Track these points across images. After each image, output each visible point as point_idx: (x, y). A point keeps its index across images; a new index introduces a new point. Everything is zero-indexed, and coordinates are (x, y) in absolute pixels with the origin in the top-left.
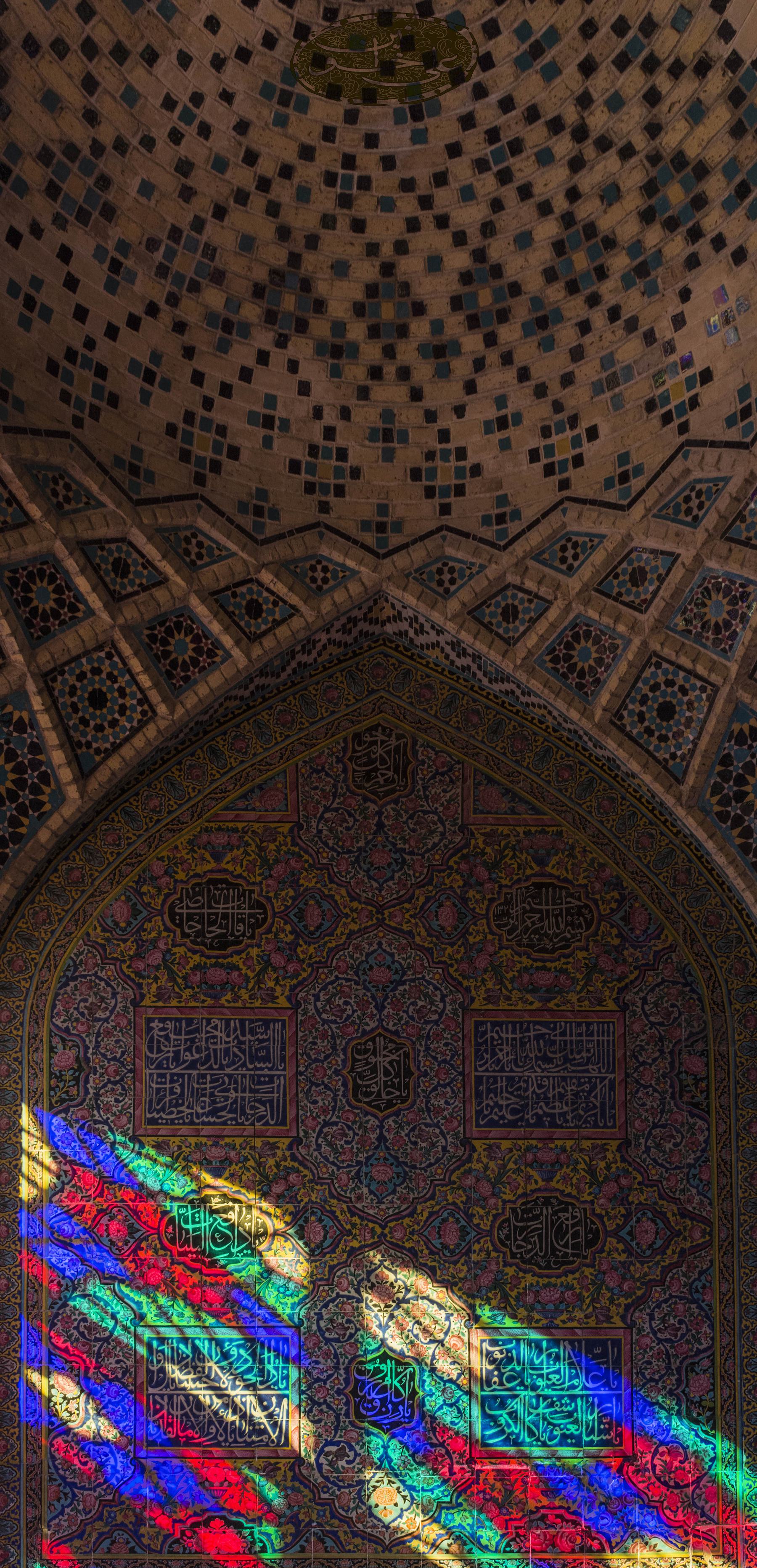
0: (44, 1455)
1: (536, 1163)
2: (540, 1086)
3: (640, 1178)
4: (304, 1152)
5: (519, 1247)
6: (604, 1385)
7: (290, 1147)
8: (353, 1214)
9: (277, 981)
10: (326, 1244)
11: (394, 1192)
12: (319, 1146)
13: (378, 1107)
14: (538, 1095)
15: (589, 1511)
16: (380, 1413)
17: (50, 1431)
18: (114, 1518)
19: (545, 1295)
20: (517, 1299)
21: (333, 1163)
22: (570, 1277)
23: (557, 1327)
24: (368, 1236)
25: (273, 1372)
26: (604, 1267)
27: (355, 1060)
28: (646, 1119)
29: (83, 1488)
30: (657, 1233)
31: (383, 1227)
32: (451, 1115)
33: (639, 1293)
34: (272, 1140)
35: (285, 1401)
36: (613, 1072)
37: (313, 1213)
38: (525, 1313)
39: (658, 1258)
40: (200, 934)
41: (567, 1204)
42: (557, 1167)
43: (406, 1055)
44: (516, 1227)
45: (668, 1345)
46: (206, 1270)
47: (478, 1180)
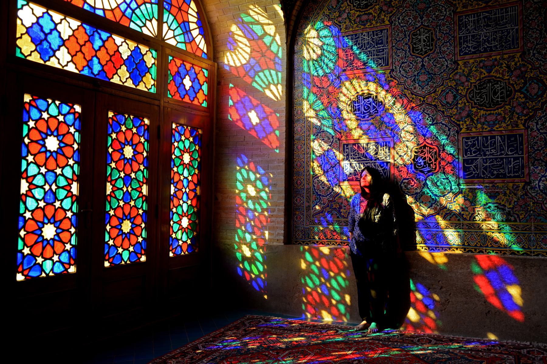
1: (485, 67)
2: (485, 37)
4: (395, 74)
5: (477, 100)
6: (516, 153)
7: (390, 73)
8: (412, 94)
9: (385, 16)
11: (428, 85)
12: (400, 71)
13: (421, 54)
14: (485, 40)
15: (510, 204)
16: (423, 167)
19: (489, 118)
20: (477, 121)
21: (405, 77)
22: (500, 110)
23: (494, 130)
24: (418, 102)
26: (515, 105)
27: (413, 38)
28: (533, 42)
30: (539, 88)
31: (424, 98)
32: (449, 53)
33: (531, 114)
36: (518, 25)
39: (540, 99)
40: (359, 4)
41: (498, 81)
42: (493, 67)
43: (432, 33)
44: (476, 93)
46: (362, 119)
47: (460, 76)
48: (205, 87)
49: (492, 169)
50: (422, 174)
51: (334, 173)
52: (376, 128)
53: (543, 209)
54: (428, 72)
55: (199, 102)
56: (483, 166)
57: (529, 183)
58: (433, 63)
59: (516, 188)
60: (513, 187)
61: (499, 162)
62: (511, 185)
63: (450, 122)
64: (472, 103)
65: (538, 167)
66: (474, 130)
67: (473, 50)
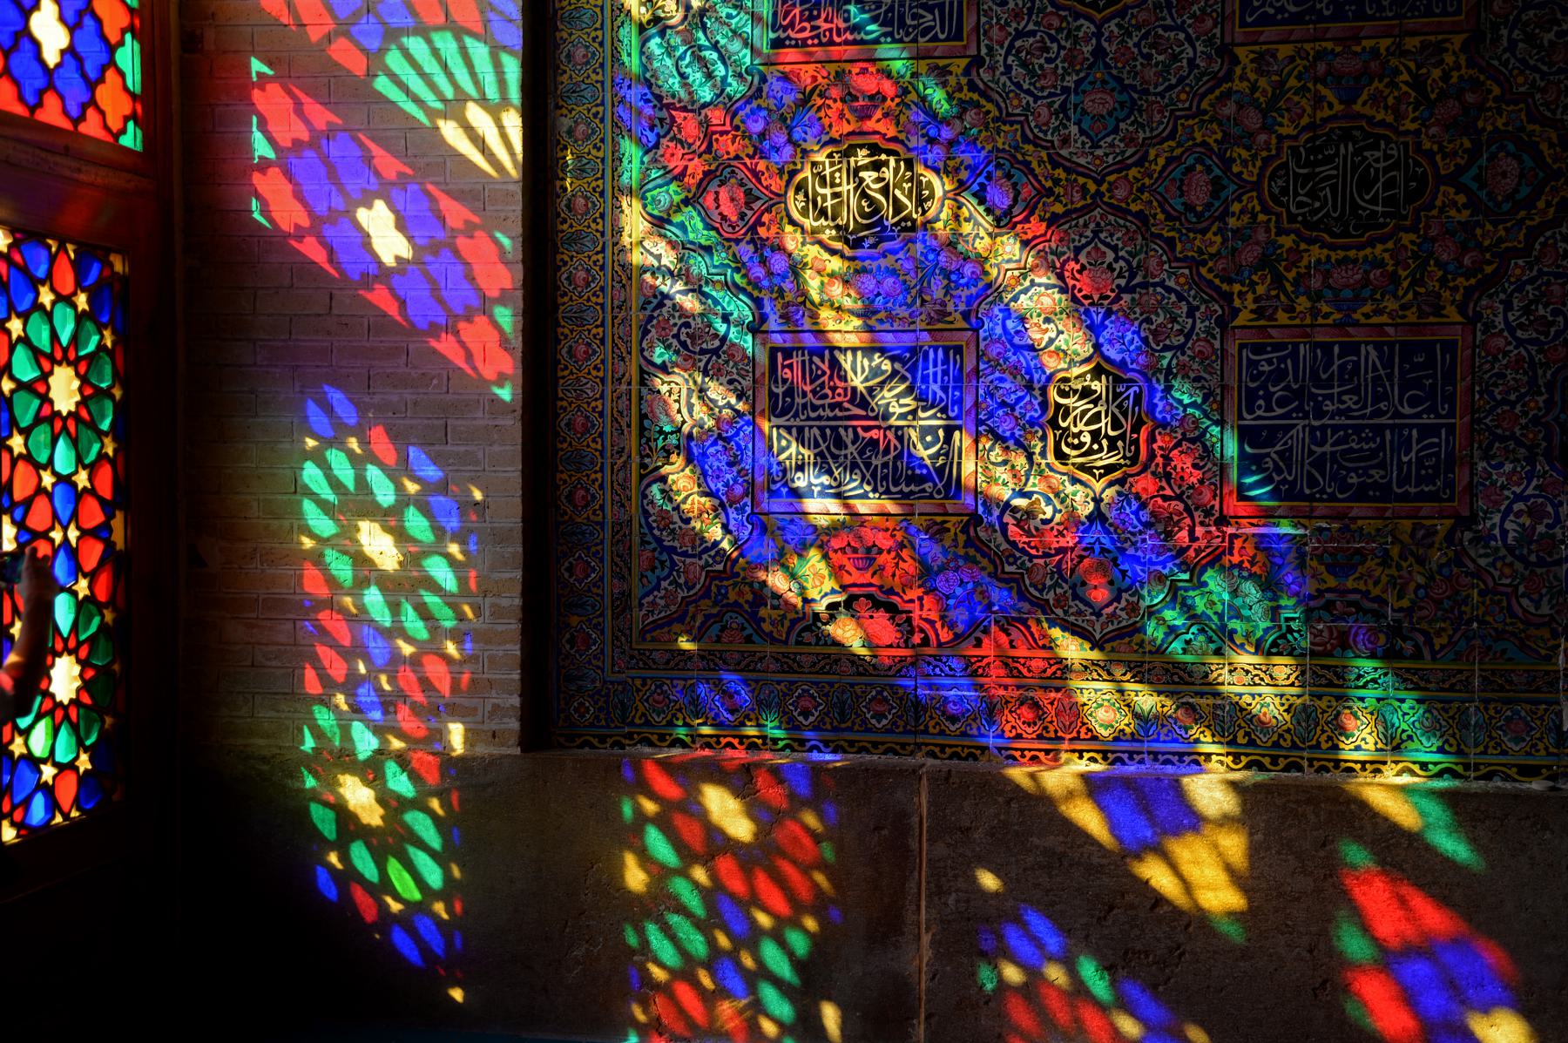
0: (634, 509)
3: (1497, 91)
4: (986, 77)
6: (1428, 411)
7: (967, 72)
8: (1055, 165)
10: (1016, 211)
11: (1116, 130)
12: (1008, 68)
15: (1400, 597)
16: (1090, 452)
17: (642, 477)
18: (725, 596)
20: (1296, 283)
21: (1028, 92)
22: (1380, 247)
23: (1356, 324)
24: (1077, 196)
25: (940, 393)
26: (1433, 232)
29: (685, 554)
30: (1522, 175)
32: (1202, 10)
33: (1488, 269)
34: (942, 63)
35: (957, 434)
37: (999, 166)
38: (1309, 305)
39: (1523, 213)
41: (1379, 137)
45: (1533, 349)
47: (1240, 107)
48: (128, 57)
49: (1341, 467)
50: (1084, 477)
51: (730, 464)
52: (908, 290)
53: (1513, 615)
54: (1119, 80)
55: (106, 128)
56: (1311, 453)
57: (1470, 521)
58: (1137, 45)
59: (1424, 537)
60: (1412, 535)
61: (1367, 440)
62: (1407, 524)
63: (1197, 282)
64: (1279, 216)
65: (1501, 465)
66: (1282, 317)
67: (1293, 9)
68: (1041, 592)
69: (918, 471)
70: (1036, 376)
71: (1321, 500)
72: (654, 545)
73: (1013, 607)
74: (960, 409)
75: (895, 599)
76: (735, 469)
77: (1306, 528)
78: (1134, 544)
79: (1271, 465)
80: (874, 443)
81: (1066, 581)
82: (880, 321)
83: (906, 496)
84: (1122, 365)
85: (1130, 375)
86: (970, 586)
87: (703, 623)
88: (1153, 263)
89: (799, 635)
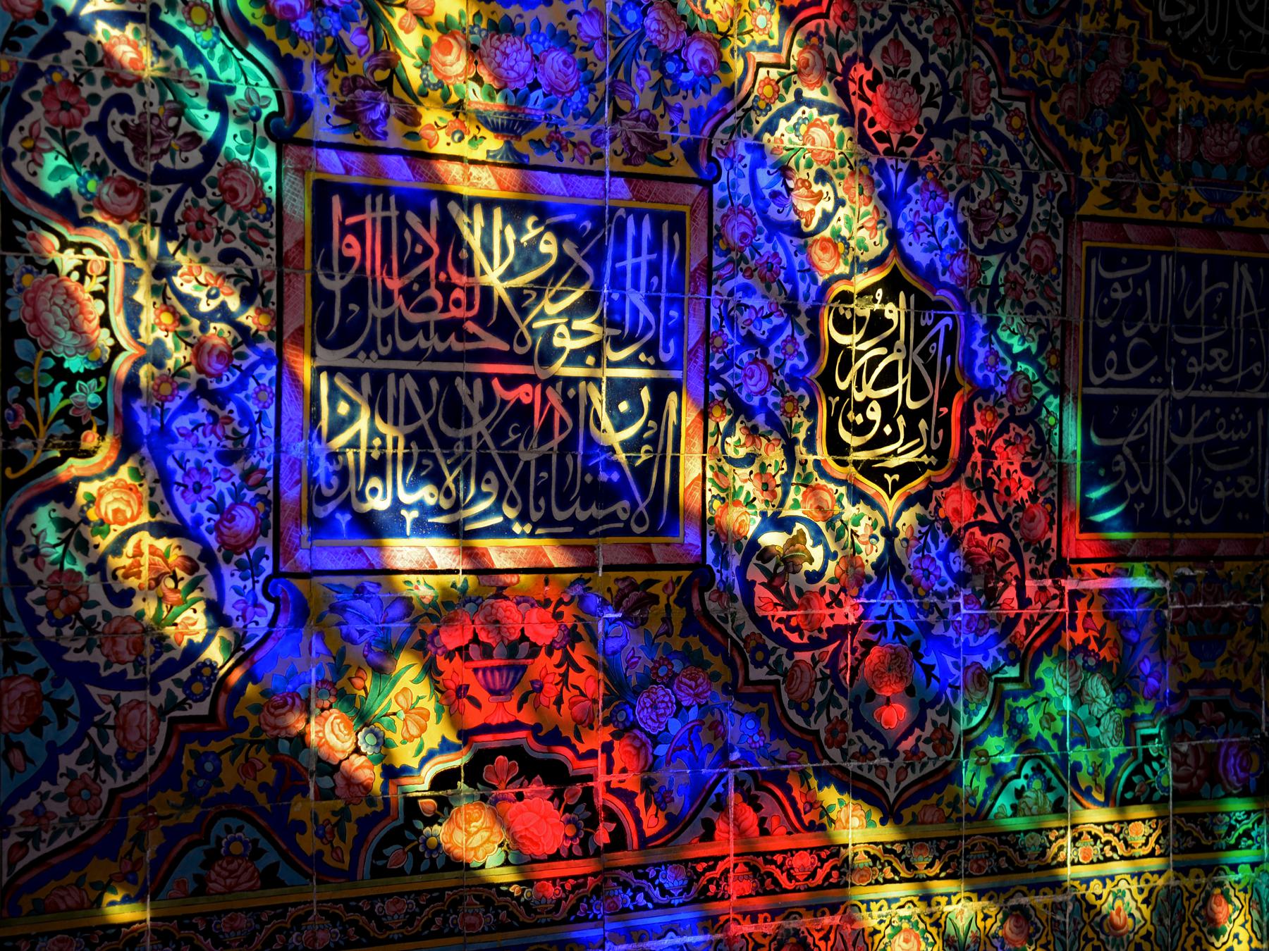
16: (880, 440)
18: (214, 778)
23: (1229, 226)
25: (645, 312)
29: (118, 682)
49: (1208, 472)
50: (871, 488)
51: (226, 457)
52: (590, 83)
56: (1172, 446)
66: (1142, 204)
68: (806, 715)
69: (603, 477)
70: (802, 287)
71: (1183, 529)
72: (40, 663)
73: (762, 751)
74: (679, 346)
75: (564, 753)
76: (236, 468)
77: (1165, 577)
78: (943, 615)
79: (1122, 467)
80: (522, 412)
81: (843, 692)
82: (538, 145)
83: (581, 529)
84: (929, 275)
85: (942, 295)
86: (693, 714)
87: (162, 851)
88: (976, 82)
89: (378, 854)
